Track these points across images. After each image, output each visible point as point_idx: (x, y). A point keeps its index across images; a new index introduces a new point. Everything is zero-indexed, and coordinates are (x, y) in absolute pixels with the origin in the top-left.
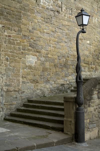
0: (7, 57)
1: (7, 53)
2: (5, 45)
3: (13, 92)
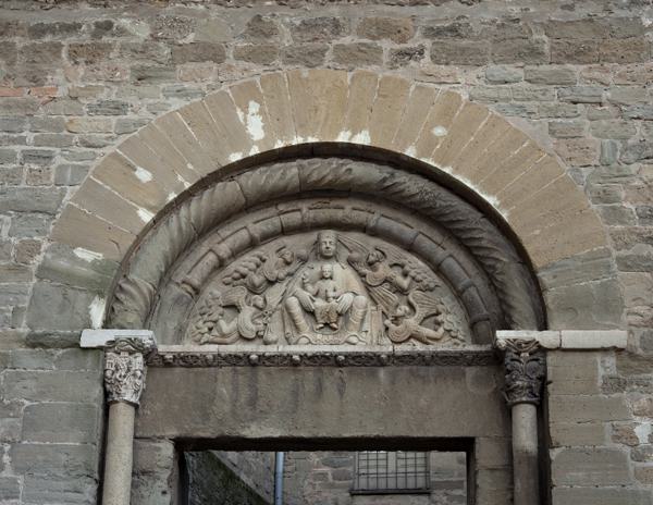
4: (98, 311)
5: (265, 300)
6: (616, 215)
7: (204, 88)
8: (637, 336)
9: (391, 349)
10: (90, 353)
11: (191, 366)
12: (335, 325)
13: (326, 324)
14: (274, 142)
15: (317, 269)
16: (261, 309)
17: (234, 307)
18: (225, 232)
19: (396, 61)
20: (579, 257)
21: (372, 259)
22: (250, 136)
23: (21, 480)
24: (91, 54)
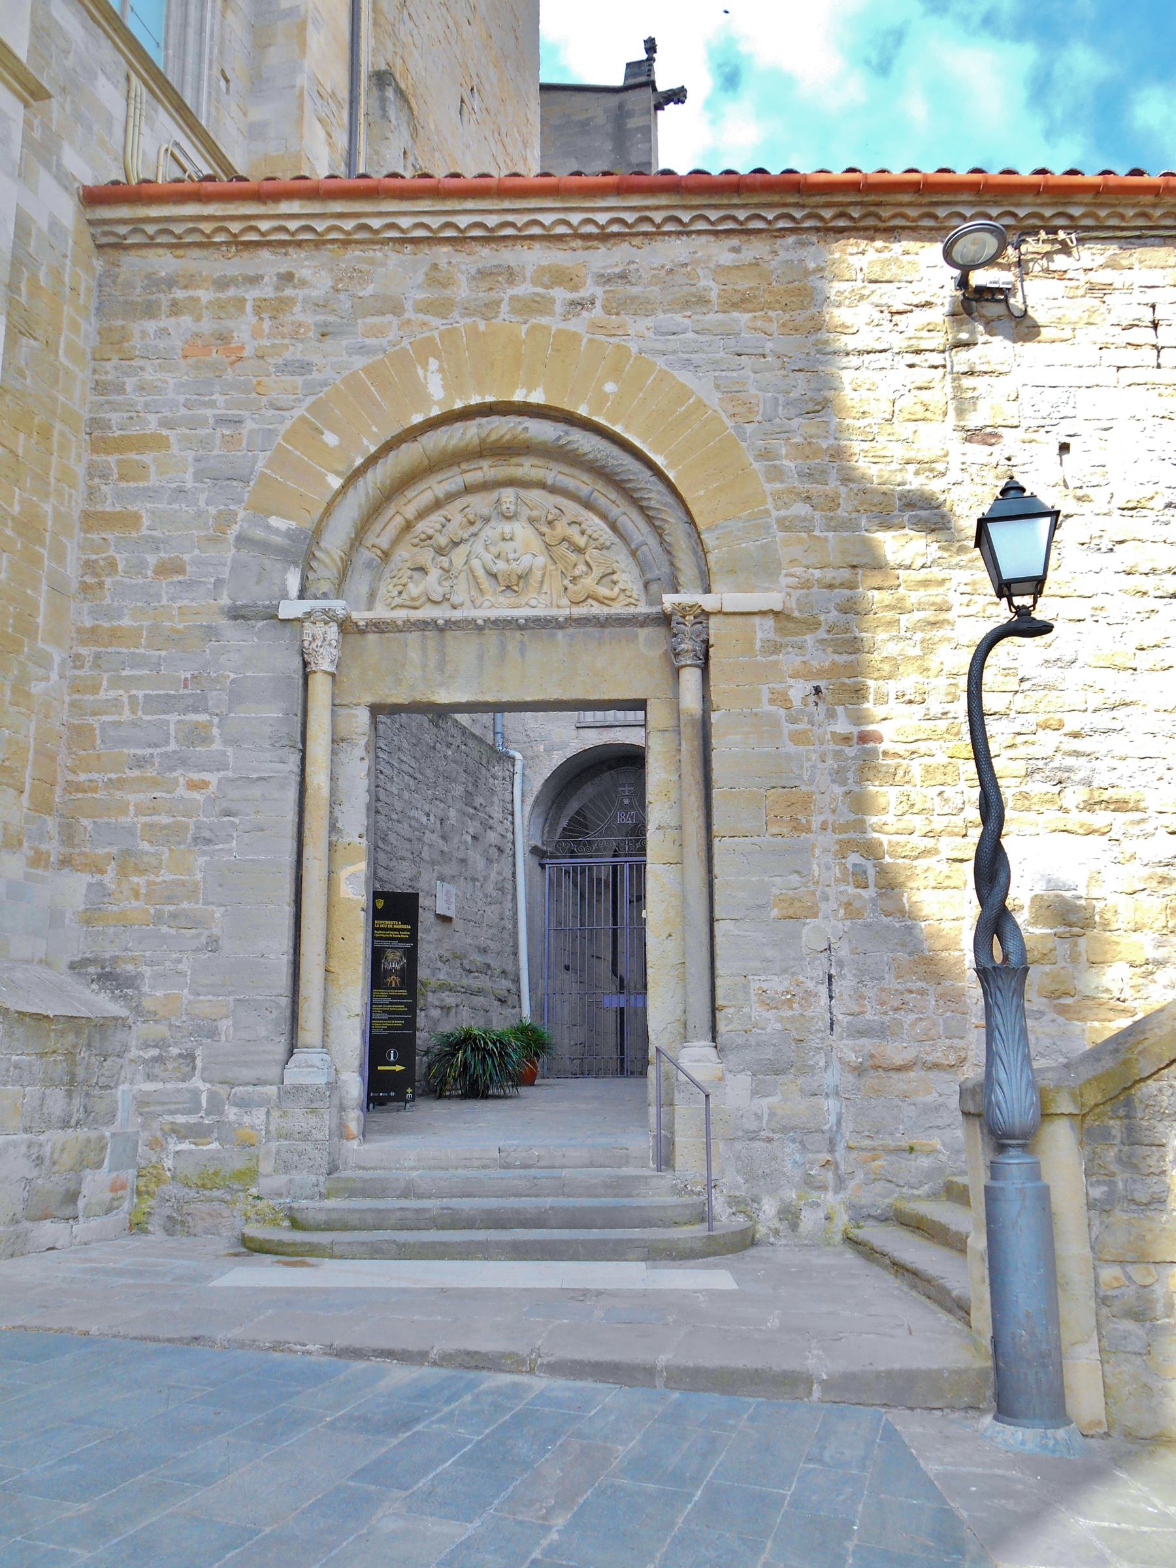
0: (854, 858)
1: (854, 836)
2: (838, 790)
3: (912, 1074)
4: (293, 581)
5: (451, 561)
6: (776, 474)
7: (385, 344)
8: (794, 599)
9: (567, 612)
10: (289, 625)
11: (383, 632)
12: (516, 588)
13: (508, 587)
14: (454, 402)
15: (499, 530)
16: (448, 571)
17: (422, 569)
18: (410, 493)
19: (569, 313)
20: (740, 518)
21: (550, 517)
22: (429, 395)
23: (230, 751)
24: (275, 308)
